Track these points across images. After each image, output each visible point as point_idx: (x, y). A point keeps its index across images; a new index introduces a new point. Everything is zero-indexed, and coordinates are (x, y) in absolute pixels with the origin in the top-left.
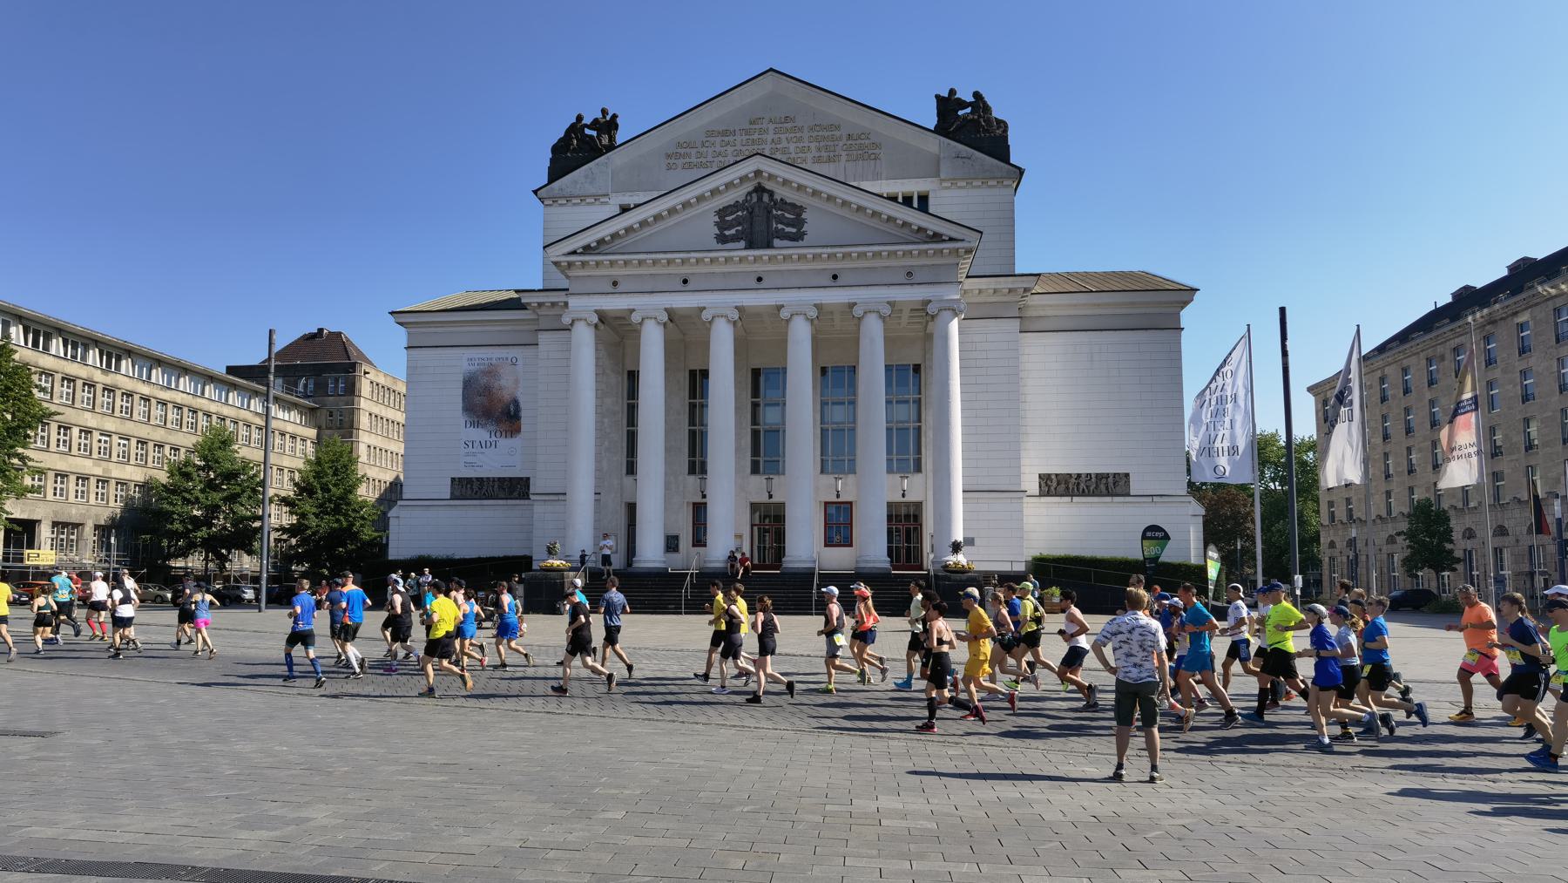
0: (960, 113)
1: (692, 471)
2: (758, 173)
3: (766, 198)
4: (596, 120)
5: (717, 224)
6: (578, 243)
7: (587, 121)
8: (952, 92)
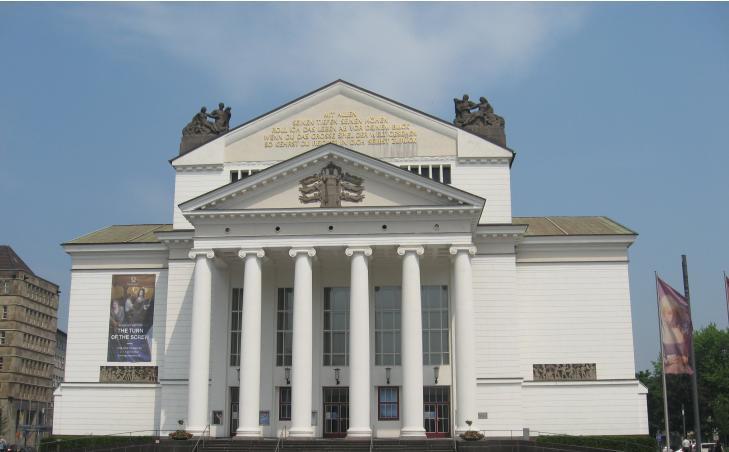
1: (279, 363)
2: (330, 156)
3: (335, 172)
4: (215, 113)
5: (300, 190)
6: (201, 204)
7: (209, 112)
8: (466, 98)
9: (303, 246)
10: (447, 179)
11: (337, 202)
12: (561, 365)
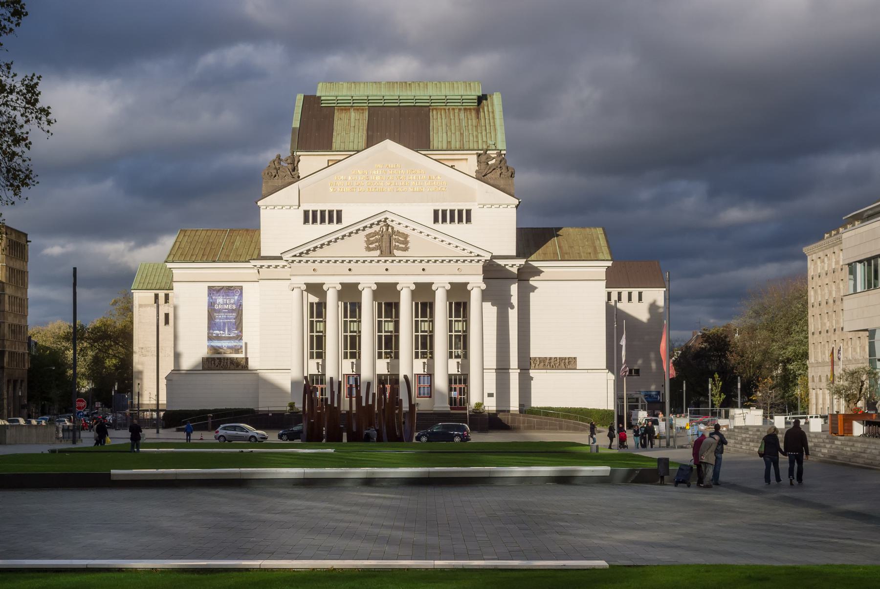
3: (390, 230)
6: (297, 252)
10: (469, 220)
12: (550, 358)
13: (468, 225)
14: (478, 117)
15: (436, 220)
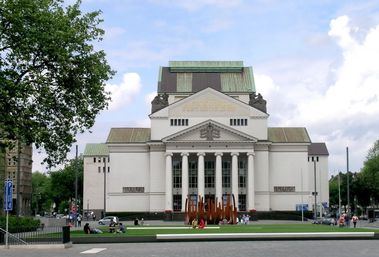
0: (255, 98)
2: (210, 123)
3: (211, 128)
5: (200, 134)
6: (169, 138)
9: (201, 152)
10: (246, 124)
11: (212, 138)
12: (283, 187)
13: (246, 127)
14: (242, 77)
15: (231, 124)
